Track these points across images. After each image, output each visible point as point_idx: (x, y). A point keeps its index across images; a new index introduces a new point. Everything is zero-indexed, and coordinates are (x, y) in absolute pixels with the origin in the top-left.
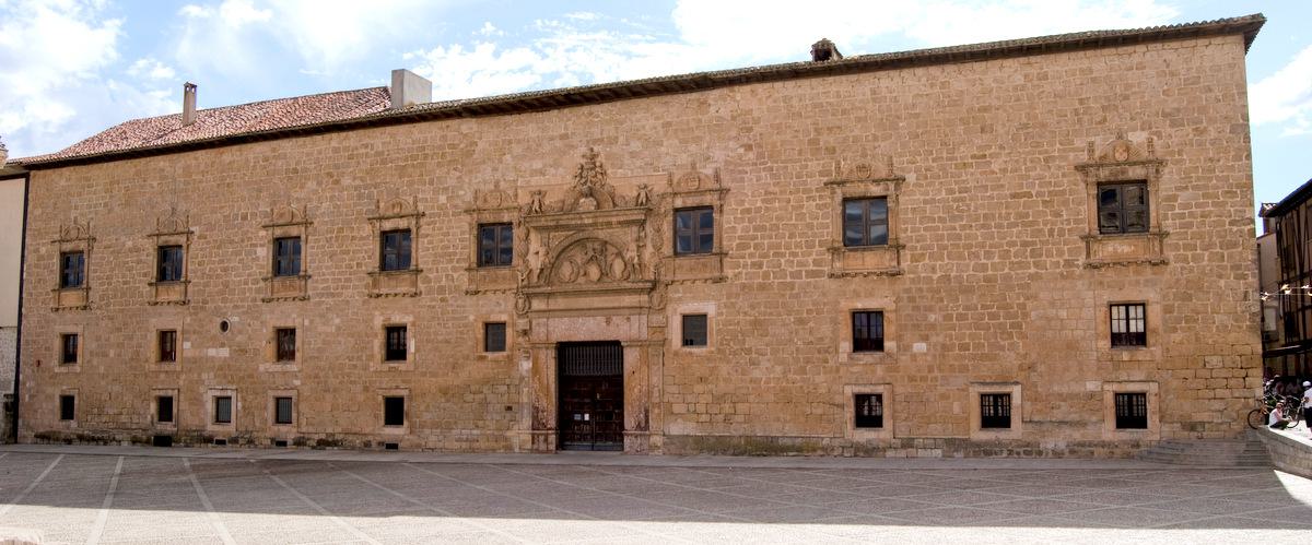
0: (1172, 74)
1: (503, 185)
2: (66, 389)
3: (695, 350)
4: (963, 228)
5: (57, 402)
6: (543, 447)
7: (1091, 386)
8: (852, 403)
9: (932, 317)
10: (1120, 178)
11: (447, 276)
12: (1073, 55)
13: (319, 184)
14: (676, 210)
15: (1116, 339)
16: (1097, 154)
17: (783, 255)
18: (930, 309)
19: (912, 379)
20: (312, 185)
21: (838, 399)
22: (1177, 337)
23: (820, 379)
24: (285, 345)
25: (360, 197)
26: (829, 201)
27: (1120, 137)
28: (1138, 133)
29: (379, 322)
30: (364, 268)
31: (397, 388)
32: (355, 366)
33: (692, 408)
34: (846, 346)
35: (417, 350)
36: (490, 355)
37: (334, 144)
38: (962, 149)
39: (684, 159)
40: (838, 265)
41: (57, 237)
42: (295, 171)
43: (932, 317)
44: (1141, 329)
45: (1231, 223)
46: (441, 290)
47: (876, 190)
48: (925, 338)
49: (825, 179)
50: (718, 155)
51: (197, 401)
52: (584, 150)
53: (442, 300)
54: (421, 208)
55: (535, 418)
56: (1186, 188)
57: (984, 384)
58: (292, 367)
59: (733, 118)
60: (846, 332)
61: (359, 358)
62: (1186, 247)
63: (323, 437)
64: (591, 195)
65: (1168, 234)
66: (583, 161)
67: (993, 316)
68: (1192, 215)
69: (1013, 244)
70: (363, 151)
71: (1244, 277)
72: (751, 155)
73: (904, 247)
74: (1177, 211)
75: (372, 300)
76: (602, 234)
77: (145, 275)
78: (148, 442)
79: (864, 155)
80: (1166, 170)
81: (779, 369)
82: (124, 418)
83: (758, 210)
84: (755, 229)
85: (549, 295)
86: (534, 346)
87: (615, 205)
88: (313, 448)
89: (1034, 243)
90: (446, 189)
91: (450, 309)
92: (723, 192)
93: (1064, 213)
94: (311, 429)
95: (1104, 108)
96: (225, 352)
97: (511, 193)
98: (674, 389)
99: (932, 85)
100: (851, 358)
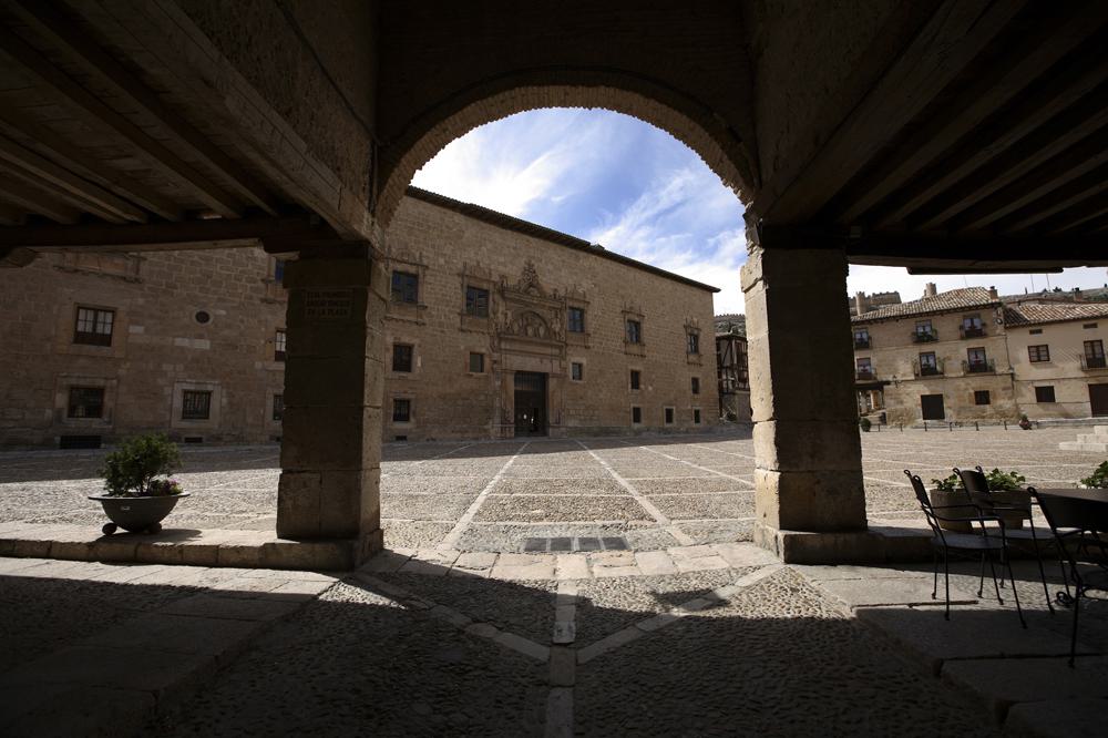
9: (654, 376)
23: (622, 400)
29: (390, 340)
31: (405, 392)
43: (654, 376)
46: (441, 325)
53: (442, 332)
72: (597, 290)
76: (538, 311)
90: (445, 255)
98: (570, 402)
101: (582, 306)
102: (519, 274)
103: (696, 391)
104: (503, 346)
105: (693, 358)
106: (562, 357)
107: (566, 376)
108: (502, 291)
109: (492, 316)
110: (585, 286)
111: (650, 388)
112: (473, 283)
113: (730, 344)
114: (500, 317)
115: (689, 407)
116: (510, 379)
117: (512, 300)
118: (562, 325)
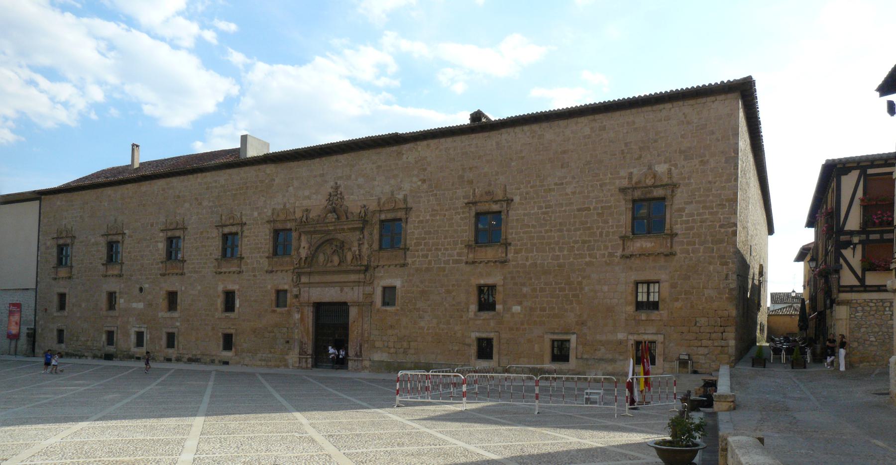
0: (688, 123)
1: (288, 206)
2: (59, 325)
3: (388, 308)
4: (547, 231)
5: (55, 333)
6: (304, 365)
7: (621, 336)
8: (475, 343)
9: (525, 290)
10: (648, 196)
12: (623, 113)
13: (191, 205)
14: (382, 222)
15: (640, 306)
16: (634, 180)
17: (440, 250)
18: (524, 284)
19: (511, 329)
20: (187, 205)
21: (468, 341)
22: (678, 304)
23: (457, 328)
24: (172, 299)
26: (468, 215)
27: (650, 168)
28: (662, 165)
29: (220, 288)
33: (386, 344)
34: (473, 307)
35: (240, 305)
36: (278, 310)
37: (199, 180)
38: (549, 179)
39: (387, 189)
40: (471, 256)
41: (55, 236)
42: (179, 197)
43: (525, 290)
44: (656, 299)
45: (721, 226)
46: (254, 269)
47: (495, 207)
48: (520, 303)
49: (466, 201)
50: (407, 186)
51: (127, 334)
52: (332, 184)
54: (244, 220)
55: (301, 348)
56: (692, 202)
57: (554, 333)
58: (176, 315)
59: (416, 162)
60: (474, 298)
62: (689, 243)
63: (190, 356)
64: (335, 212)
65: (676, 234)
66: (331, 190)
67: (561, 290)
68: (694, 221)
69: (576, 242)
71: (726, 264)
72: (425, 186)
73: (510, 244)
74: (684, 218)
76: (339, 236)
77: (101, 259)
78: (101, 357)
79: (490, 185)
80: (679, 190)
81: (435, 321)
82: (89, 343)
83: (427, 221)
84: (426, 233)
85: (310, 274)
87: (347, 218)
88: (185, 363)
89: (590, 241)
90: (257, 208)
92: (408, 210)
93: (610, 221)
94: (185, 352)
95: (641, 149)
96: (141, 305)
97: (292, 210)
99: (533, 137)
100: (475, 315)
102: (324, 201)
116: (309, 313)
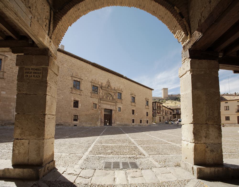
11: (87, 93)
25: (69, 70)
29: (73, 99)
30: (69, 86)
31: (77, 113)
32: (67, 108)
35: (81, 106)
39: (118, 85)
46: (86, 95)
48: (137, 113)
59: (123, 82)
61: (68, 106)
70: (69, 61)
72: (125, 88)
75: (71, 94)
76: (110, 93)
86: (102, 108)
90: (87, 76)
91: (87, 99)
98: (117, 117)
101: (121, 92)
102: (106, 83)
103: (147, 115)
104: (101, 102)
105: (147, 107)
106: (116, 105)
107: (116, 111)
108: (101, 87)
109: (99, 94)
110: (122, 87)
111: (137, 114)
112: (94, 85)
113: (156, 104)
114: (101, 94)
115: (146, 119)
116: (103, 111)
117: (104, 90)
118: (116, 97)
